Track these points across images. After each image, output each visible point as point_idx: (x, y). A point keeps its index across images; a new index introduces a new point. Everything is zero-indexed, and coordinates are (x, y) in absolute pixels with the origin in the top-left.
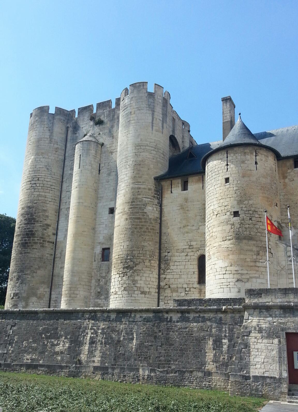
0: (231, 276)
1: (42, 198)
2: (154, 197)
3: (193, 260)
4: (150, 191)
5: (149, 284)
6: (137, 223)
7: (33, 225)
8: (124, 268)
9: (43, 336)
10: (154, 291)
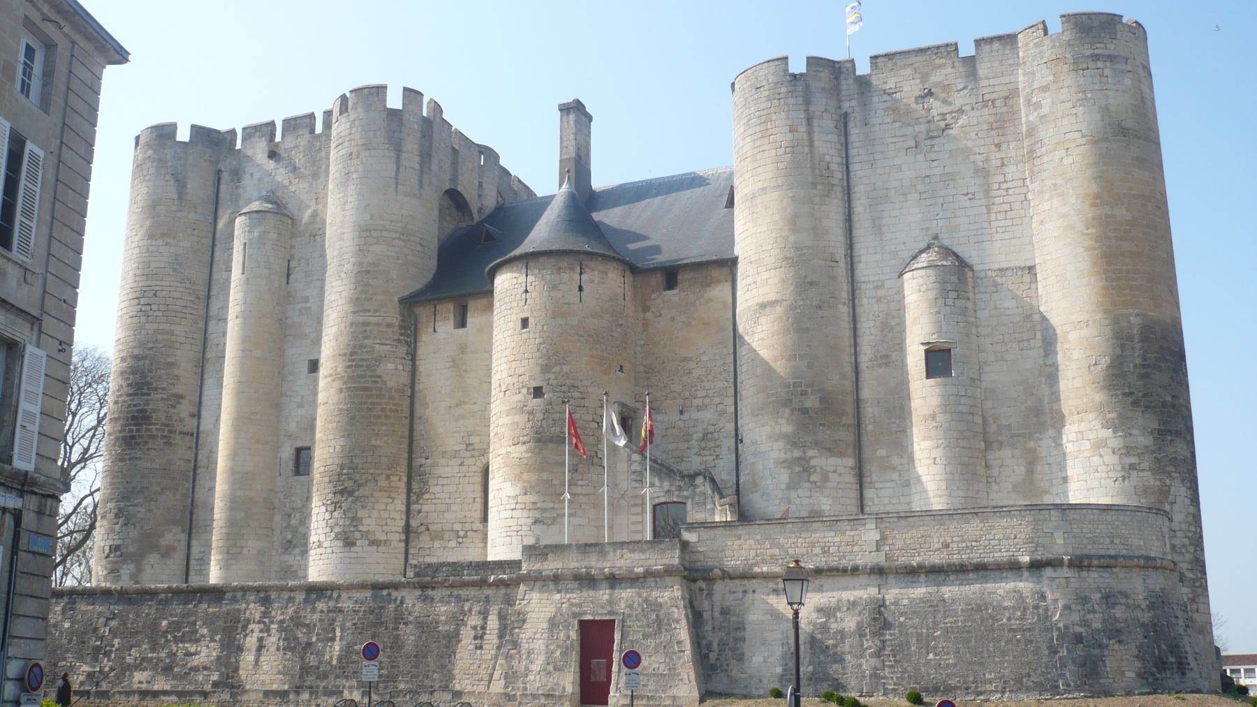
0: (525, 513)
1: (165, 337)
2: (399, 341)
3: (473, 474)
4: (390, 330)
5: (386, 524)
6: (362, 398)
7: (145, 397)
8: (335, 493)
9: (169, 636)
10: (397, 538)
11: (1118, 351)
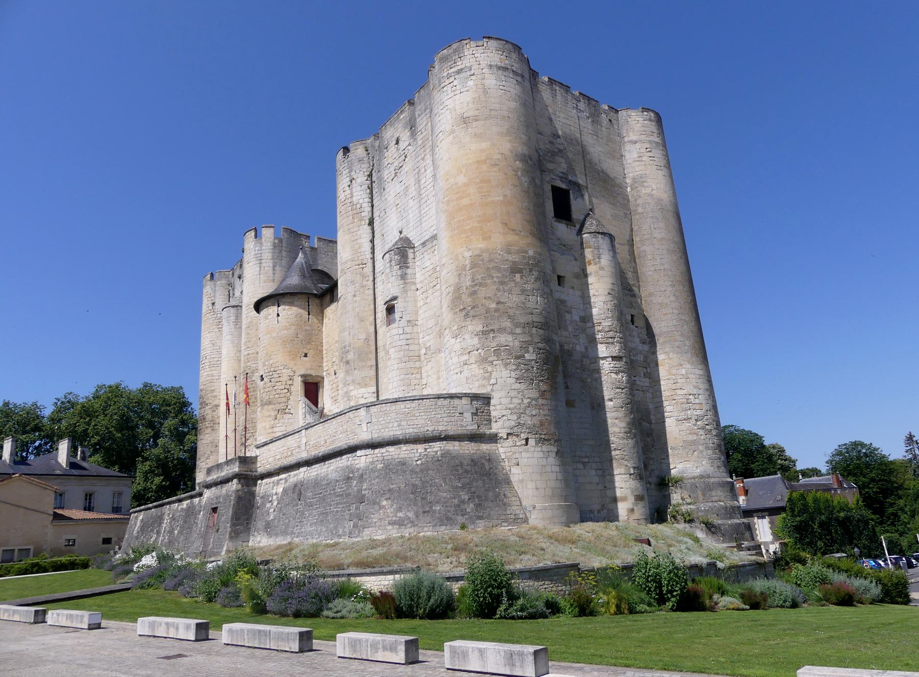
1: (210, 378)
11: (457, 280)
